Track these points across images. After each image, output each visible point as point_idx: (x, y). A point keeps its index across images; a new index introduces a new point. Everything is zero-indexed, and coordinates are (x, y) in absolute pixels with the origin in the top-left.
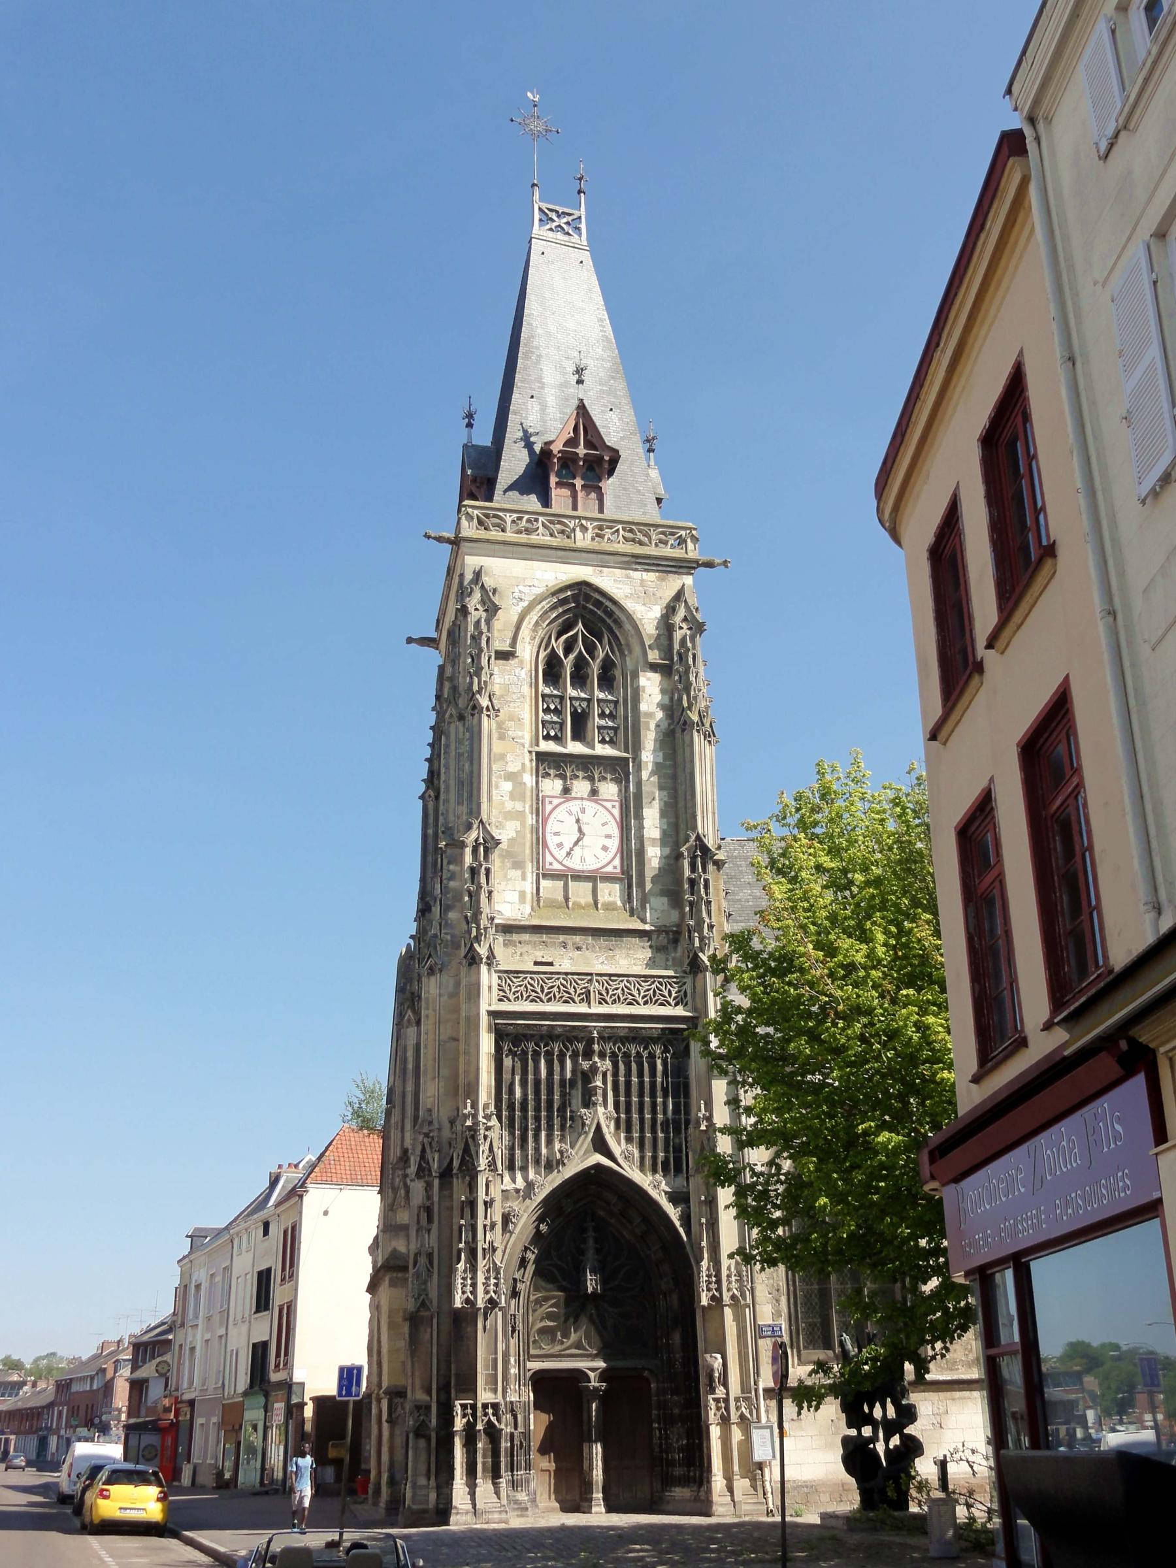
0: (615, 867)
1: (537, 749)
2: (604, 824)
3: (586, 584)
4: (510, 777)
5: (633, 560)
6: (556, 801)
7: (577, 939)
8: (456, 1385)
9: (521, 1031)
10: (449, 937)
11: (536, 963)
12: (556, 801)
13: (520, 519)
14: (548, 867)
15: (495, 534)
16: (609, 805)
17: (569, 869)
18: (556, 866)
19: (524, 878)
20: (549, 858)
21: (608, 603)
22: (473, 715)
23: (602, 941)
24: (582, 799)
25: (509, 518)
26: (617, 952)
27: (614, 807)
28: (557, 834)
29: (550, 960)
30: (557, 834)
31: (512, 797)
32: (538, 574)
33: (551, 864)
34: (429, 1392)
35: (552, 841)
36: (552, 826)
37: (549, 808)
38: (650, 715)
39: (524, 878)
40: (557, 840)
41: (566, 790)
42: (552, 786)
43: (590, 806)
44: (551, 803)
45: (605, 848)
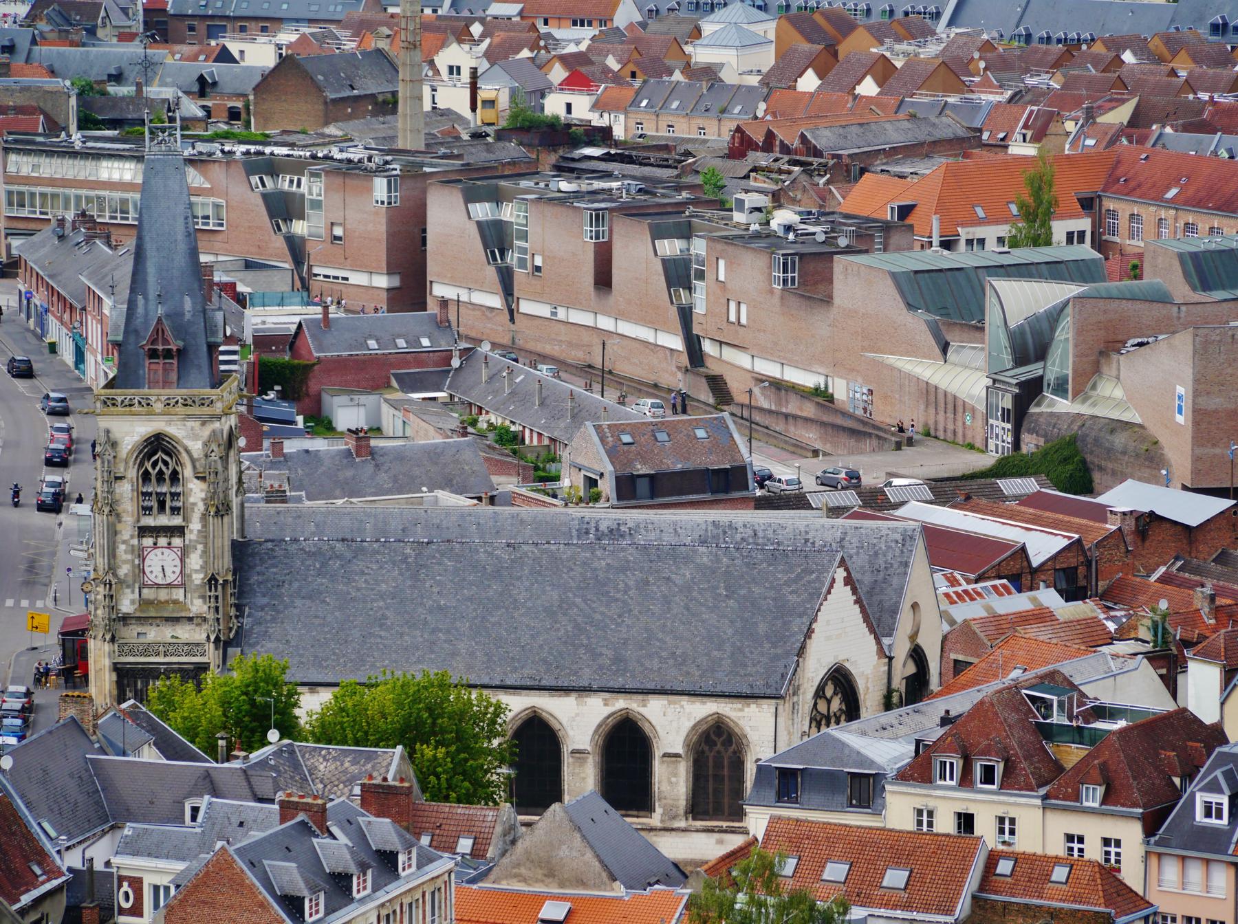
1: (139, 525)
4: (124, 542)
6: (149, 550)
7: (158, 621)
16: (175, 550)
18: (150, 582)
19: (133, 592)
20: (146, 579)
31: (126, 552)
35: (147, 570)
36: (147, 562)
37: (145, 553)
38: (194, 504)
39: (133, 592)
40: (150, 569)
42: (148, 541)
45: (174, 572)
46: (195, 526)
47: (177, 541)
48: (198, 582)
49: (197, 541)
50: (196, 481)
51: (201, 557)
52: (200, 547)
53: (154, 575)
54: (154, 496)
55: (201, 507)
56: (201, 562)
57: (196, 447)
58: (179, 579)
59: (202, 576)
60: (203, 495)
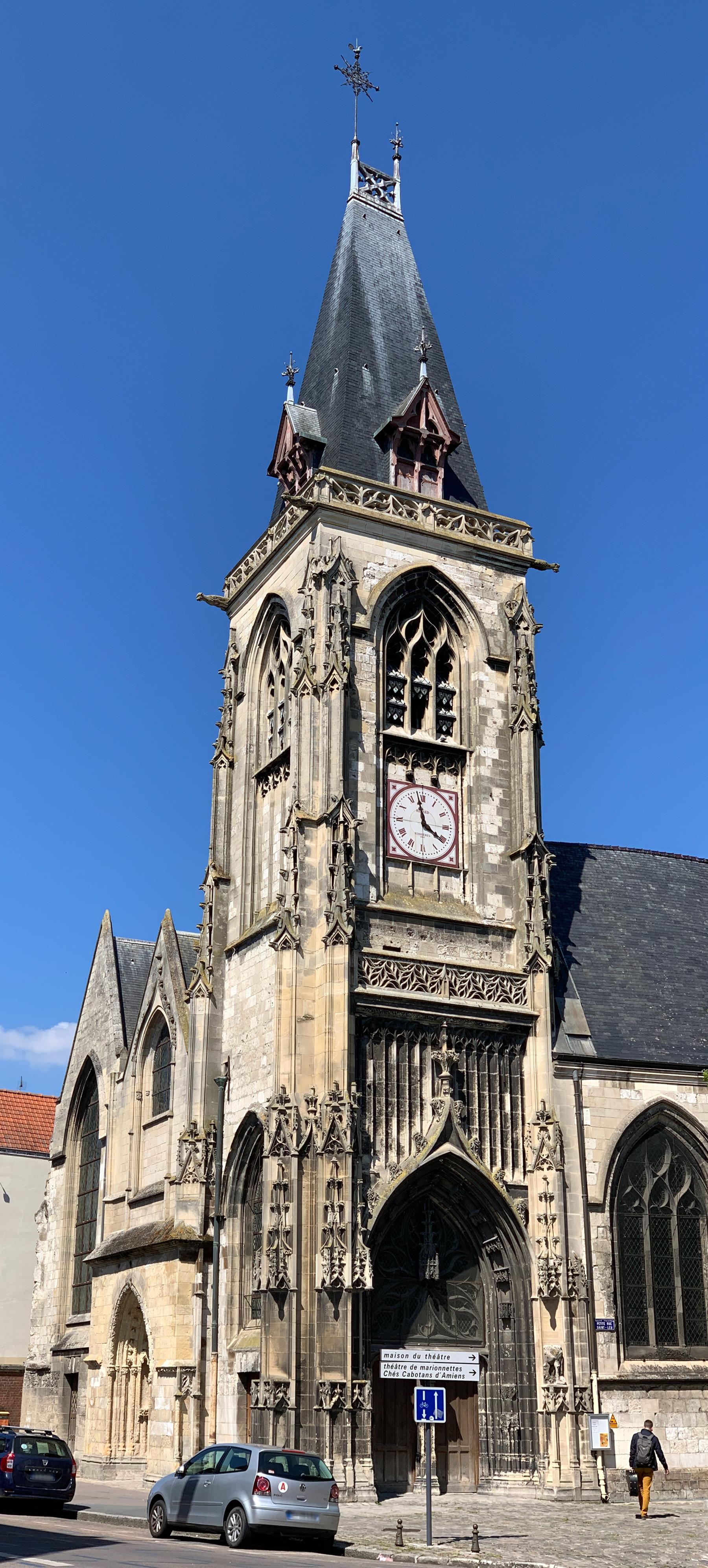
0: (451, 859)
2: (442, 815)
3: (432, 569)
5: (475, 551)
8: (321, 1364)
9: (377, 1015)
10: (305, 913)
11: (385, 948)
12: (399, 787)
13: (372, 494)
14: (391, 852)
15: (346, 505)
16: (446, 796)
17: (411, 857)
18: (399, 852)
21: (451, 592)
22: (332, 690)
23: (444, 933)
24: (423, 787)
25: (362, 491)
26: (458, 944)
27: (451, 798)
28: (400, 819)
29: (398, 946)
30: (400, 819)
32: (388, 553)
33: (394, 849)
34: (286, 1369)
35: (395, 826)
37: (392, 792)
41: (410, 777)
42: (397, 771)
43: (431, 797)
44: (394, 787)
46: (489, 751)
47: (447, 780)
48: (494, 860)
49: (491, 780)
50: (487, 668)
51: (499, 812)
52: (497, 792)
53: (406, 838)
54: (407, 687)
55: (497, 718)
56: (498, 821)
57: (489, 610)
58: (453, 854)
59: (501, 849)
60: (501, 697)
